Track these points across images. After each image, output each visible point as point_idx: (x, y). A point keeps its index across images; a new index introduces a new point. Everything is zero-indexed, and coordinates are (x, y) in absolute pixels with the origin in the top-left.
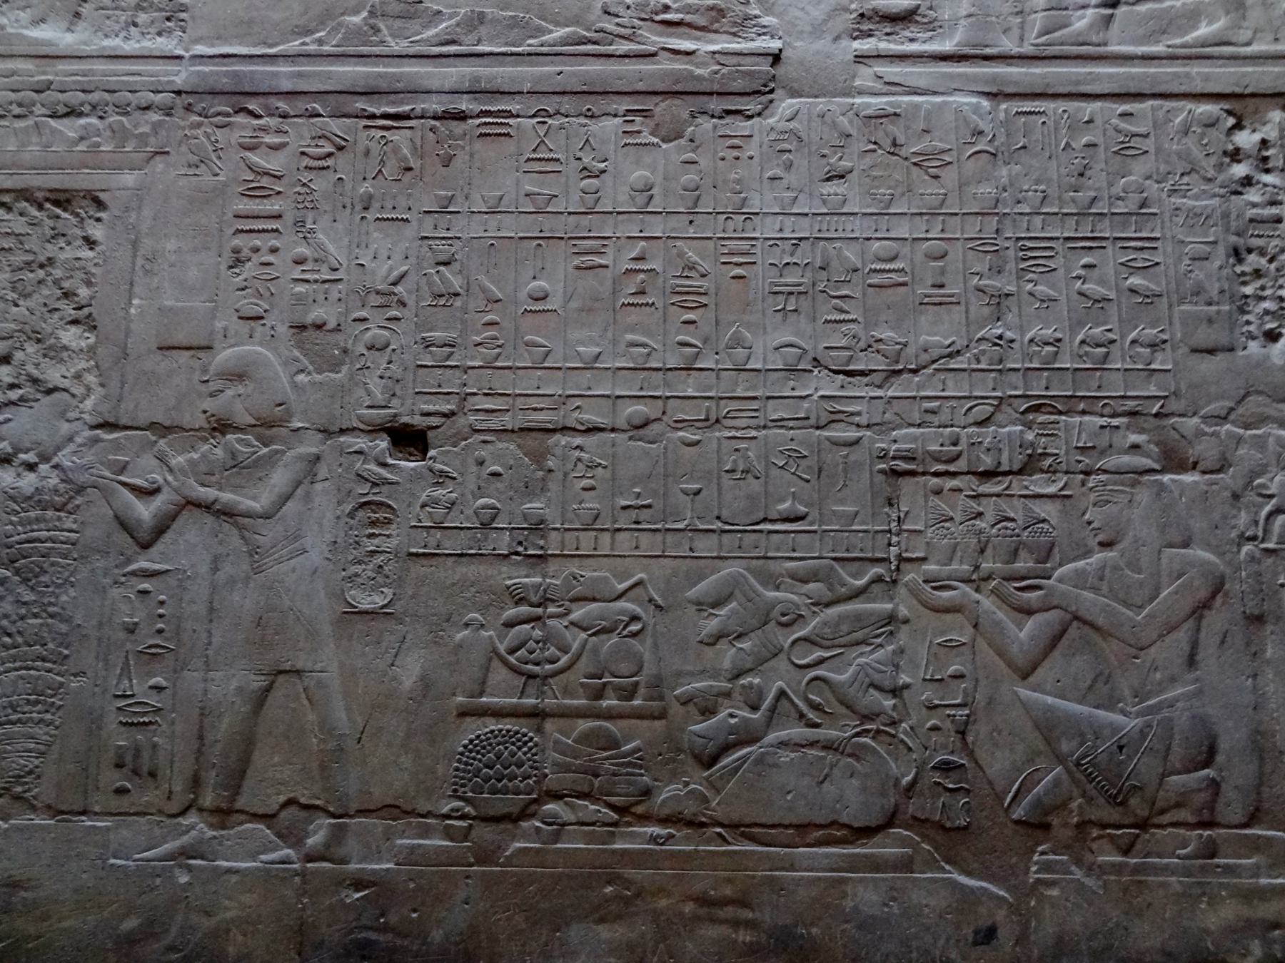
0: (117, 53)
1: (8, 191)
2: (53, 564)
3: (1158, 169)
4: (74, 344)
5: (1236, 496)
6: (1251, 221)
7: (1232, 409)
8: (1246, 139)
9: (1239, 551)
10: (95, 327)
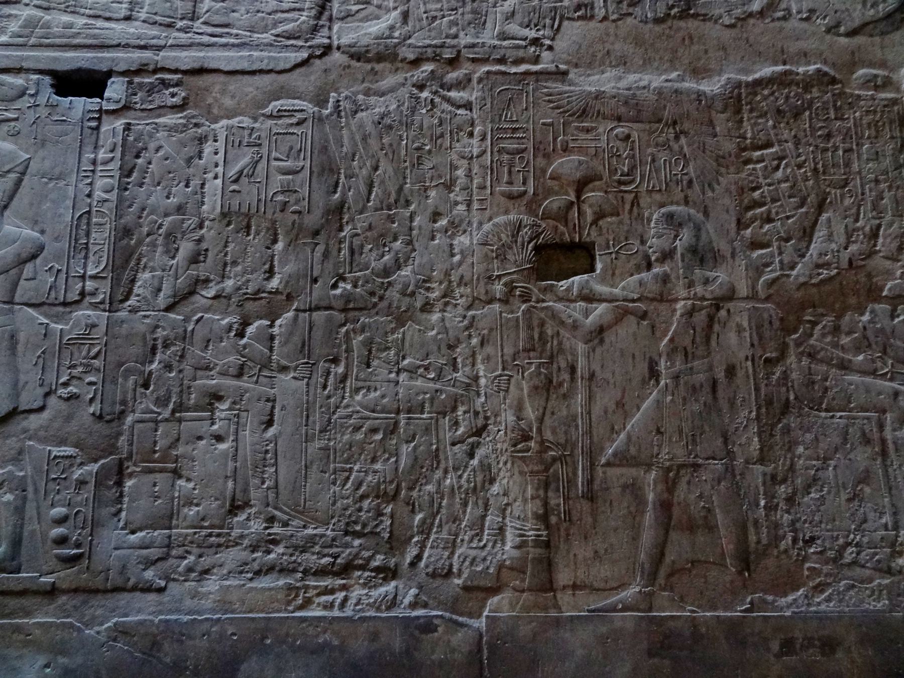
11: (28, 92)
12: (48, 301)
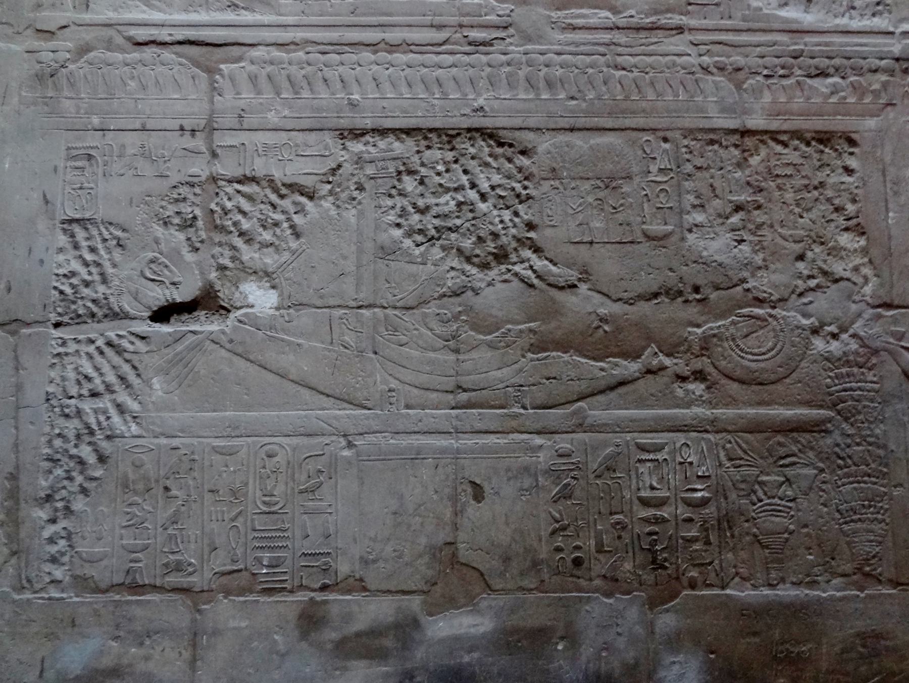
0: (850, 29)
1: (785, 132)
2: (864, 407)
4: (849, 246)
10: (863, 233)
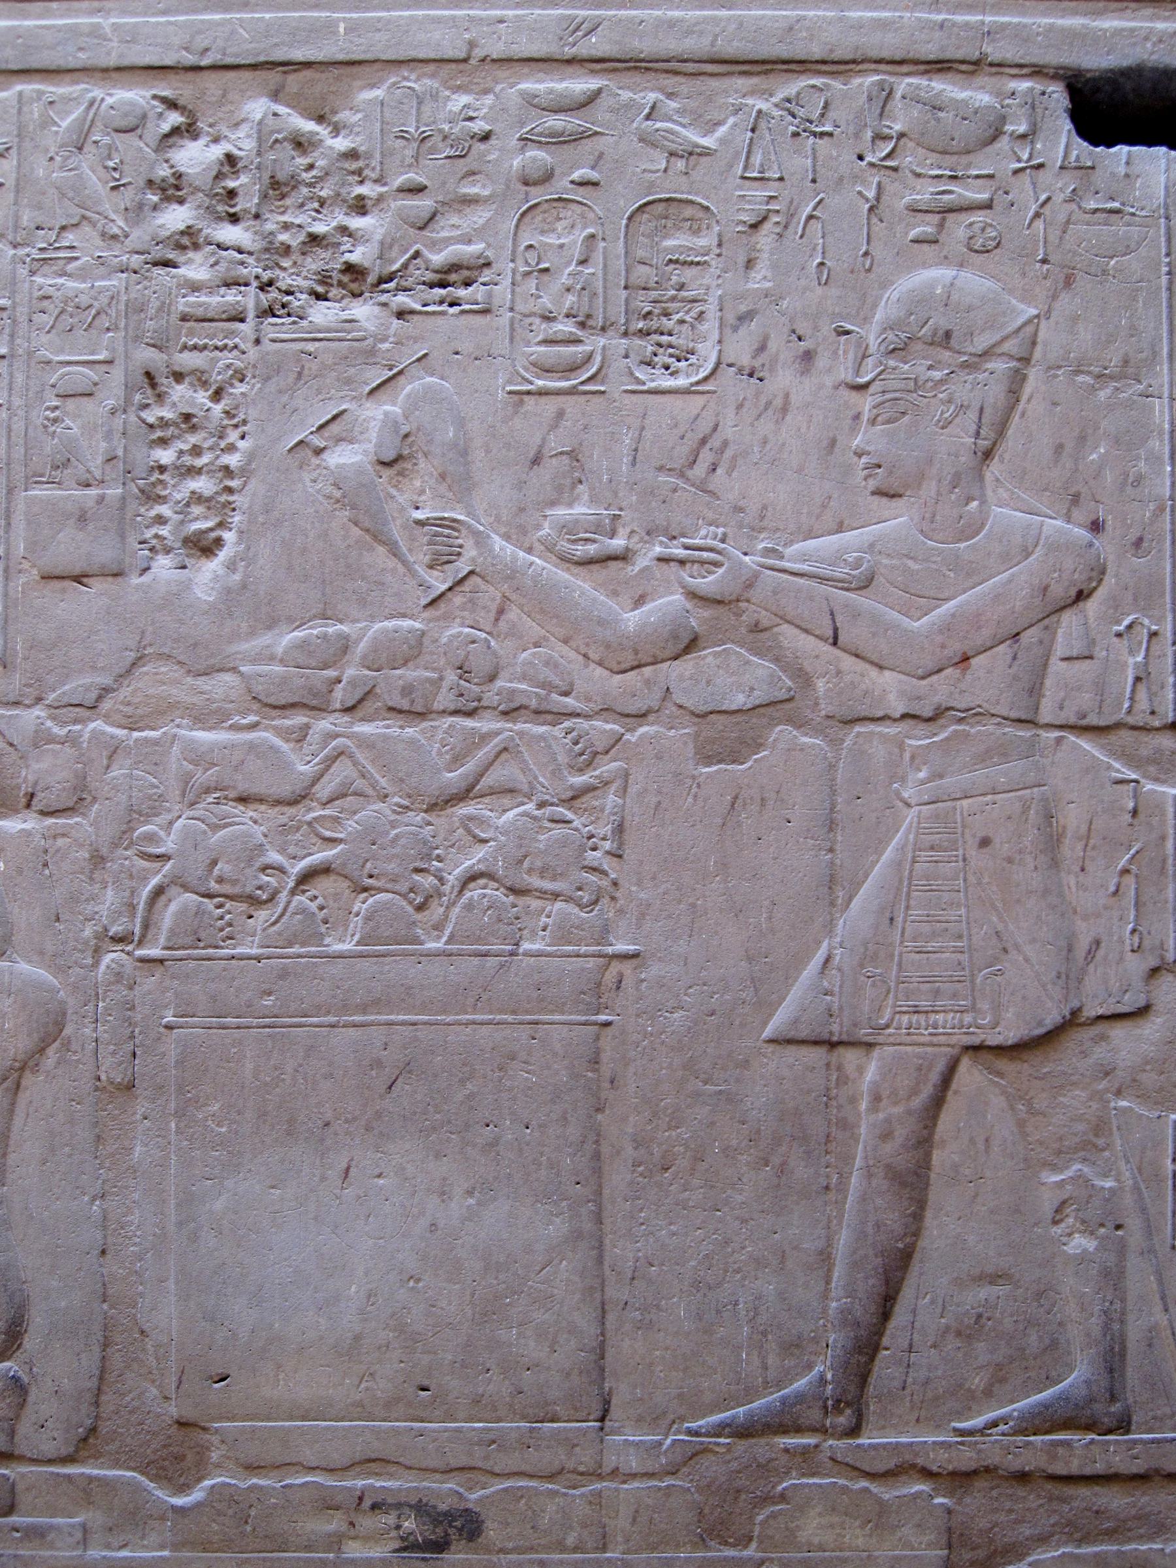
3: (17, 218)
5: (98, 860)
6: (184, 318)
7: (106, 690)
8: (196, 157)
9: (96, 964)
11: (1009, 128)
12: (1131, 720)
